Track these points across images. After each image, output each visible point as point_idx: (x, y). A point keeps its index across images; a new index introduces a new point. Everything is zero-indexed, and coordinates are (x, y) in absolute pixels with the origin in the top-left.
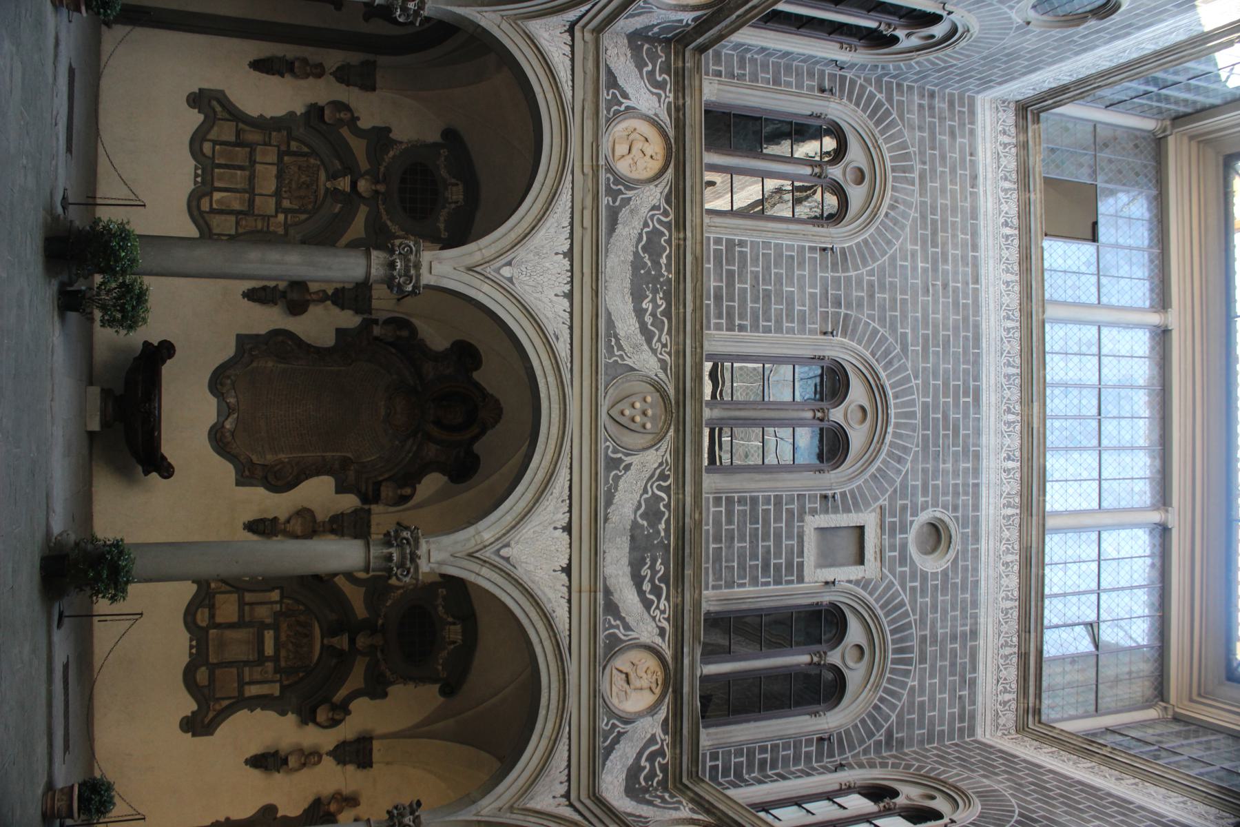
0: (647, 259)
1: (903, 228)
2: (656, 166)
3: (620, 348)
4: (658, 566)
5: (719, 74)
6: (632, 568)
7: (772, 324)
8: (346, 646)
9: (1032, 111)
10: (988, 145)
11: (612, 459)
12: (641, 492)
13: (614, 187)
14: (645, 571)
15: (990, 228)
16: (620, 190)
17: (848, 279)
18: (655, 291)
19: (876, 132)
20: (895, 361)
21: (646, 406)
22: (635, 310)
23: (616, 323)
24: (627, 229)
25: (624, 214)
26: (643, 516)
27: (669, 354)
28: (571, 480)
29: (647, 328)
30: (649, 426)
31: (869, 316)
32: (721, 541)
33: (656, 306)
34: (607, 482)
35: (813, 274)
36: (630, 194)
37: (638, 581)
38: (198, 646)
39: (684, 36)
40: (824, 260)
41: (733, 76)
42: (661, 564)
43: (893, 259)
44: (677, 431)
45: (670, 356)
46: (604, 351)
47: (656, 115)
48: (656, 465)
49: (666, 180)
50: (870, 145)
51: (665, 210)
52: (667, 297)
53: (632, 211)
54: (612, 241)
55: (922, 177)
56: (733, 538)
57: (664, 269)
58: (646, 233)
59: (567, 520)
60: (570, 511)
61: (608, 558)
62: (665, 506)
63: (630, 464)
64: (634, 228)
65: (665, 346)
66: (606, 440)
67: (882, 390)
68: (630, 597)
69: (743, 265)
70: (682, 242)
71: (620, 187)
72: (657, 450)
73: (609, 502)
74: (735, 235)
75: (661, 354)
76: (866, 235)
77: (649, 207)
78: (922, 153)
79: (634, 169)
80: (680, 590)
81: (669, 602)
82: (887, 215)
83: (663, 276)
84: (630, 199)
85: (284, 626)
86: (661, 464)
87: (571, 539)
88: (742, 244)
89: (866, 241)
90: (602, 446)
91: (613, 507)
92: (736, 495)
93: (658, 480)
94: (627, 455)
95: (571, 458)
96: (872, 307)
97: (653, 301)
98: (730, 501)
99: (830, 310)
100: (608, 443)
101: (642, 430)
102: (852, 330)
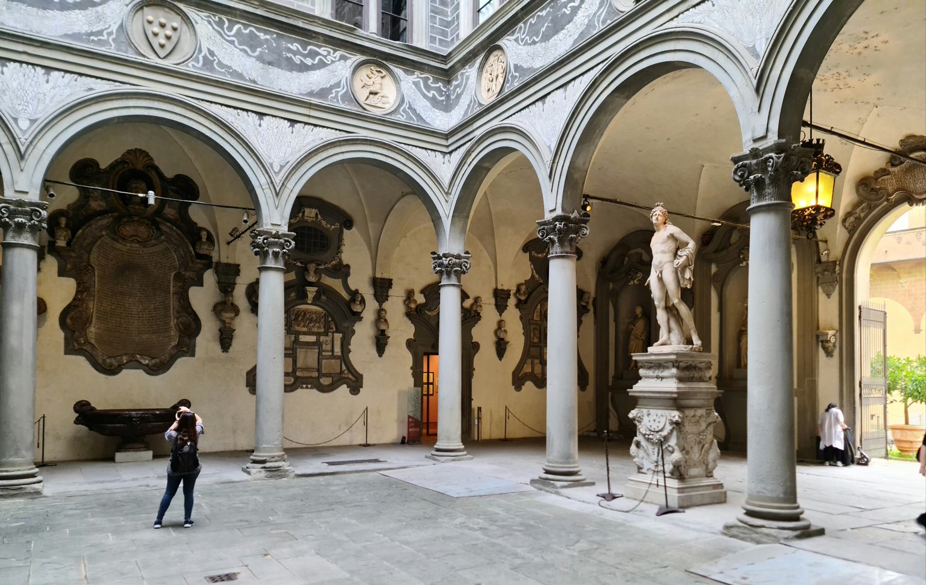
8: (315, 289)
14: (297, 59)
26: (253, 49)
34: (221, 73)
38: (307, 383)
42: (292, 45)
62: (245, 29)
63: (209, 50)
68: (315, 77)
72: (197, 23)
73: (241, 76)
80: (314, 35)
85: (297, 328)
86: (209, 23)
87: (269, 115)
91: (245, 74)
93: (223, 29)
94: (200, 51)
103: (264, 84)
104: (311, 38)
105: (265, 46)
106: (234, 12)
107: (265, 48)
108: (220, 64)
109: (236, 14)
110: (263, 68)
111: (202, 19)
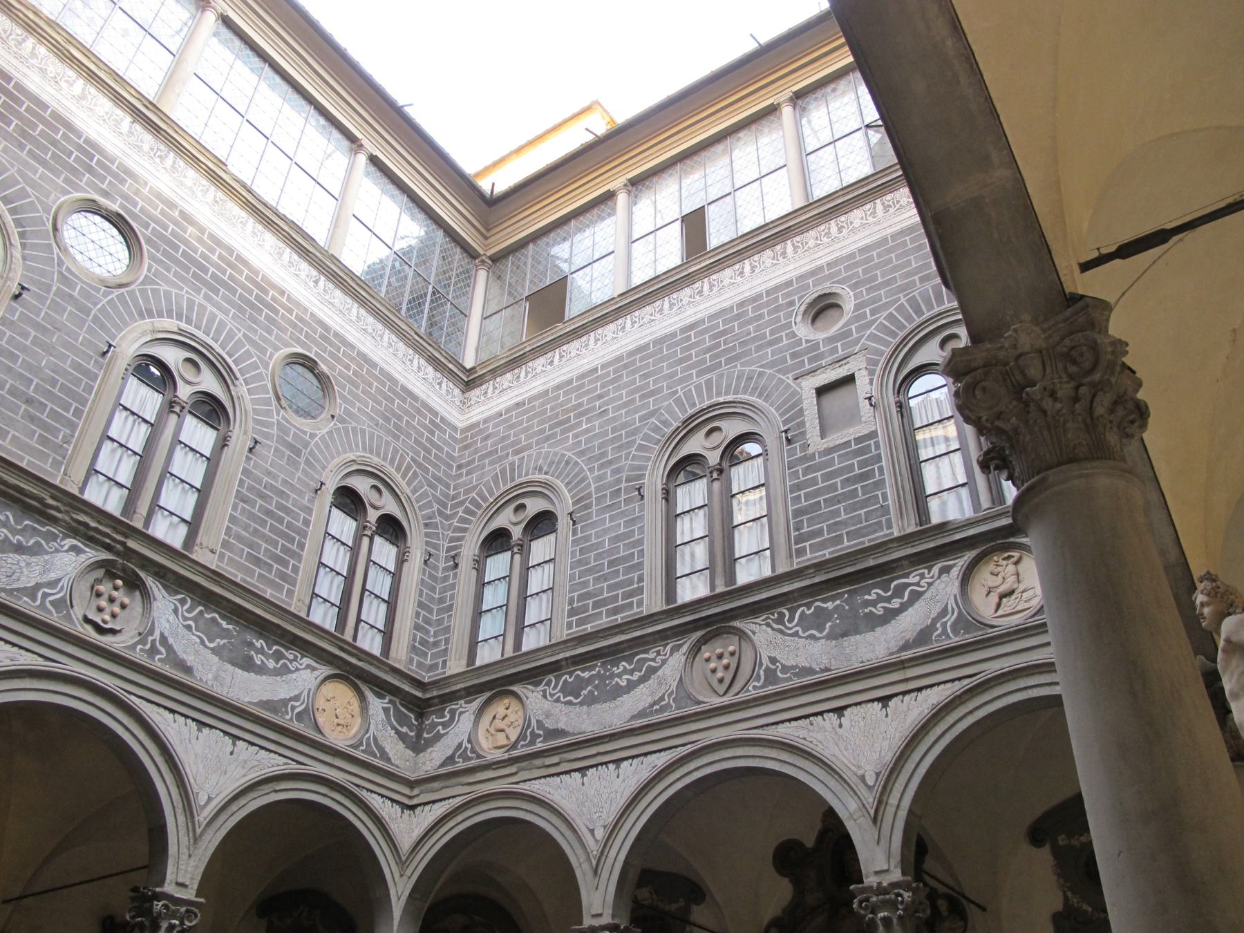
0: (585, 692)
1: (556, 454)
2: (515, 705)
3: (662, 698)
4: (873, 597)
5: (445, 662)
6: (876, 627)
7: (636, 550)
9: (468, 377)
10: (494, 403)
11: (765, 680)
12: (796, 639)
13: (529, 739)
14: (879, 611)
15: (554, 376)
16: (530, 733)
17: (598, 489)
18: (613, 676)
19: (485, 506)
20: (662, 418)
21: (714, 657)
23: (640, 708)
24: (561, 718)
25: (550, 725)
26: (820, 628)
27: (665, 646)
28: (789, 720)
29: (644, 675)
30: (731, 648)
31: (627, 459)
32: (841, 535)
33: (625, 671)
34: (789, 679)
35: (594, 524)
36: (534, 722)
37: (891, 615)
39: (409, 703)
40: (583, 519)
41: (446, 649)
43: (581, 454)
44: (734, 618)
45: (668, 644)
46: (665, 714)
47: (474, 713)
48: (769, 630)
49: (523, 690)
50: (496, 507)
51: (546, 685)
52: (616, 663)
53: (547, 717)
54: (571, 730)
55: (516, 452)
56: (836, 524)
57: (594, 672)
58: (564, 698)
59: (831, 714)
60: (821, 713)
61: (869, 656)
62: (809, 609)
63: (770, 658)
64: (561, 711)
65: (658, 653)
66: (748, 691)
67: (686, 422)
68: (908, 619)
69: (588, 595)
70: (569, 661)
71: (528, 734)
72: (754, 633)
73: (809, 671)
74: (563, 611)
75: (665, 655)
76: (562, 486)
77: (544, 700)
78: (500, 459)
79: (516, 723)
80: (894, 565)
81: (909, 573)
82: (546, 473)
83: (599, 671)
84: (538, 721)
86: (768, 625)
88: (571, 602)
89: (567, 485)
90: (752, 693)
91: (815, 666)
92: (793, 534)
93: (784, 624)
94: (761, 664)
95: (767, 725)
96: (618, 459)
97: (619, 676)
98: (800, 539)
99: (623, 497)
100: (751, 688)
101: (737, 655)
102: (639, 470)
103: (841, 667)
104: (892, 570)
105: (836, 616)
106: (791, 596)
107: (836, 619)
108: (785, 669)
109: (794, 597)
110: (836, 646)
111: (760, 625)
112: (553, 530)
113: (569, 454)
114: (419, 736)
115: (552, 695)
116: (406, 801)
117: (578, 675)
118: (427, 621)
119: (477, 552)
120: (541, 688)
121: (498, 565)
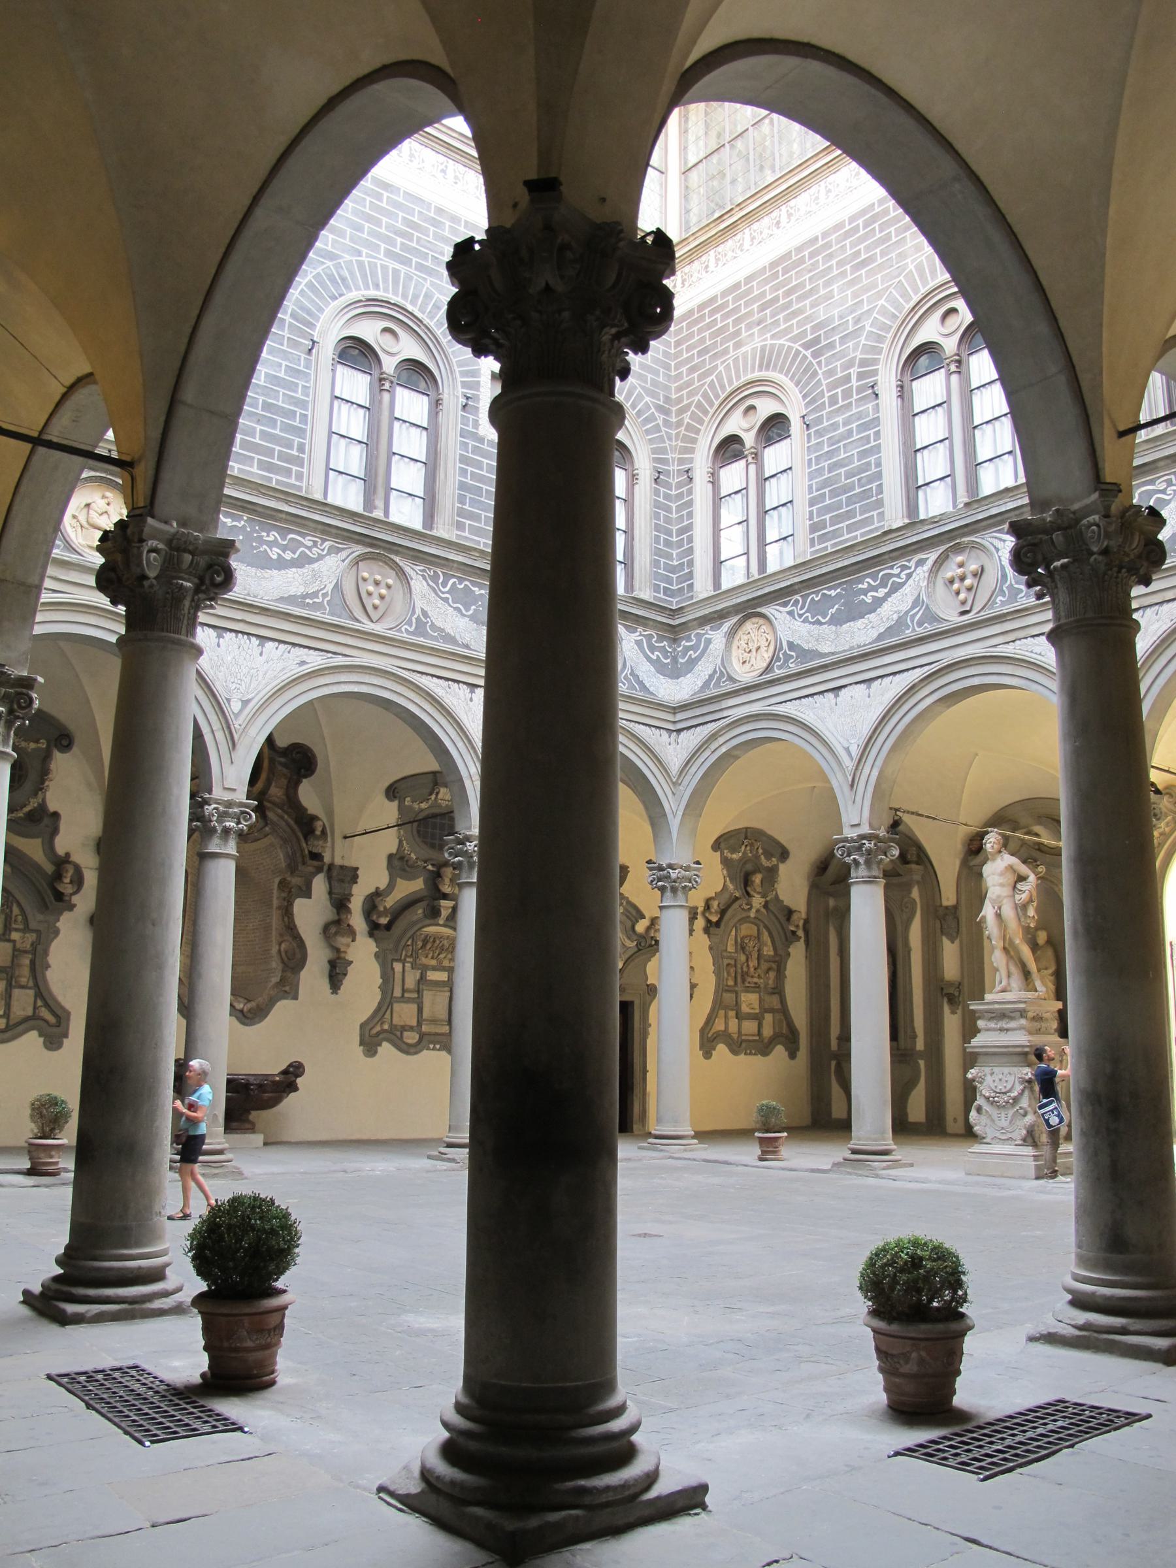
22: (874, 611)
65: (904, 568)
97: (865, 593)
112: (785, 435)
113: (796, 346)
114: (675, 659)
115: (800, 616)
116: (671, 727)
117: (824, 594)
118: (668, 543)
119: (710, 465)
120: (789, 608)
121: (734, 475)
